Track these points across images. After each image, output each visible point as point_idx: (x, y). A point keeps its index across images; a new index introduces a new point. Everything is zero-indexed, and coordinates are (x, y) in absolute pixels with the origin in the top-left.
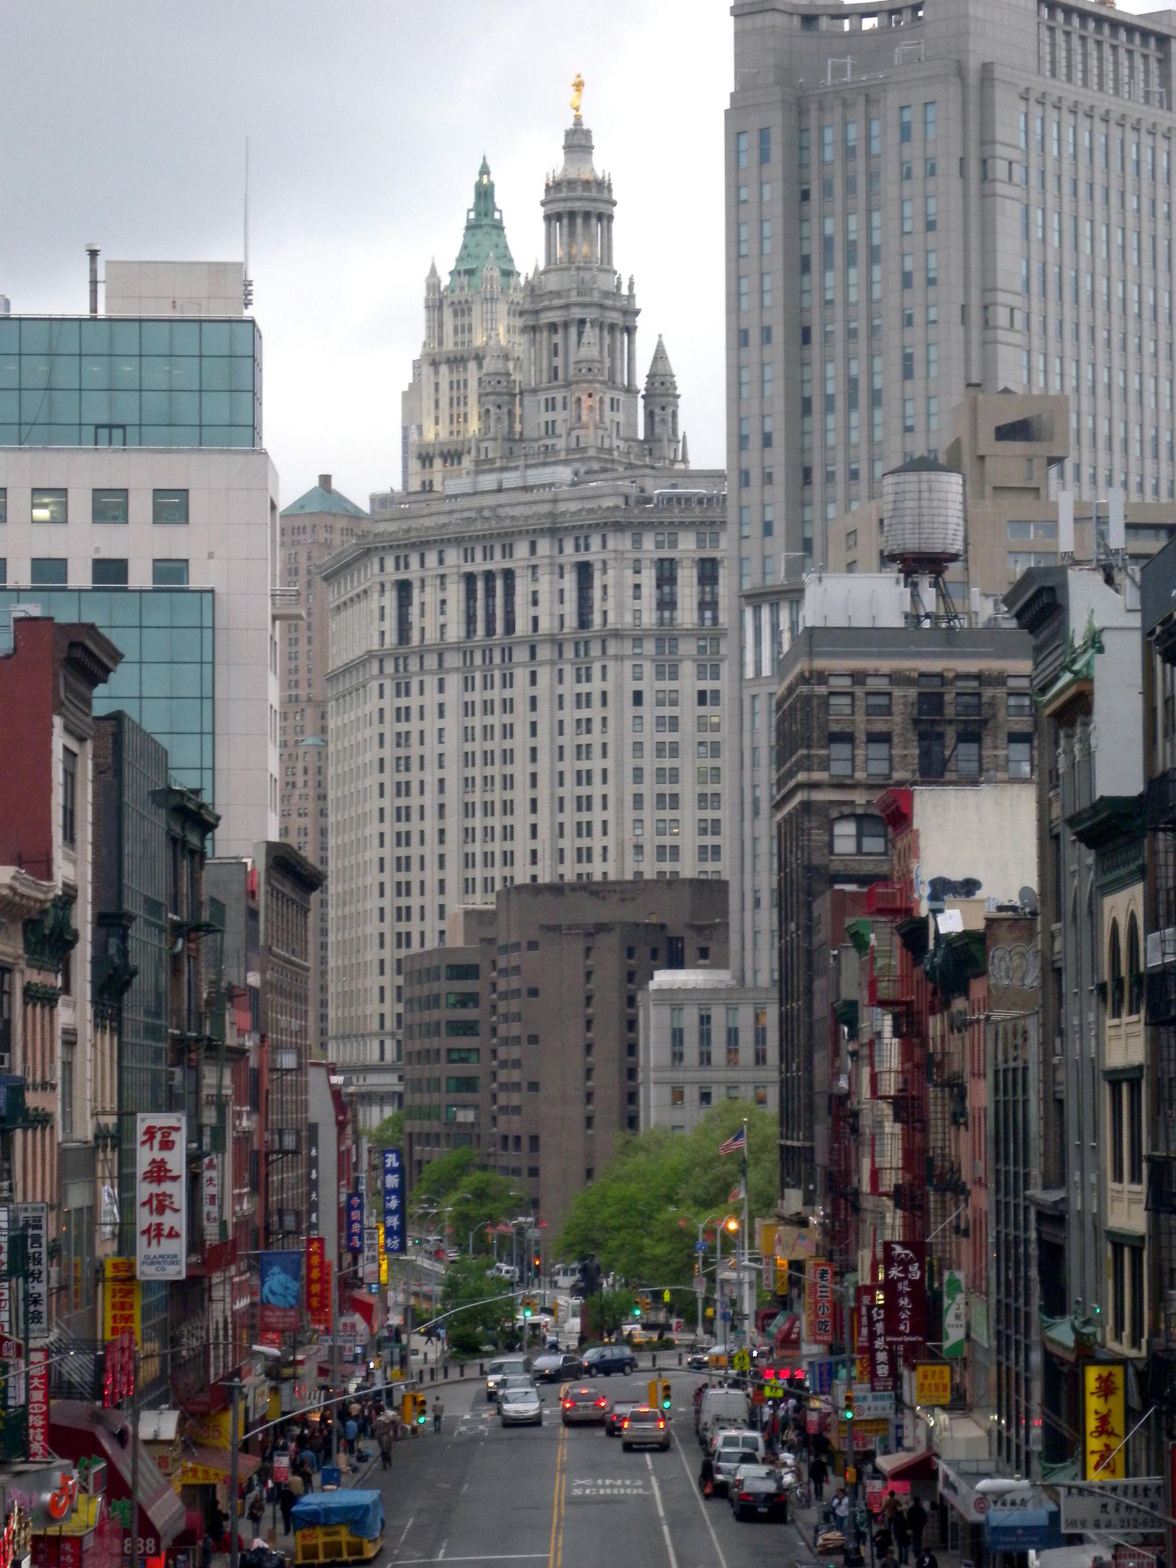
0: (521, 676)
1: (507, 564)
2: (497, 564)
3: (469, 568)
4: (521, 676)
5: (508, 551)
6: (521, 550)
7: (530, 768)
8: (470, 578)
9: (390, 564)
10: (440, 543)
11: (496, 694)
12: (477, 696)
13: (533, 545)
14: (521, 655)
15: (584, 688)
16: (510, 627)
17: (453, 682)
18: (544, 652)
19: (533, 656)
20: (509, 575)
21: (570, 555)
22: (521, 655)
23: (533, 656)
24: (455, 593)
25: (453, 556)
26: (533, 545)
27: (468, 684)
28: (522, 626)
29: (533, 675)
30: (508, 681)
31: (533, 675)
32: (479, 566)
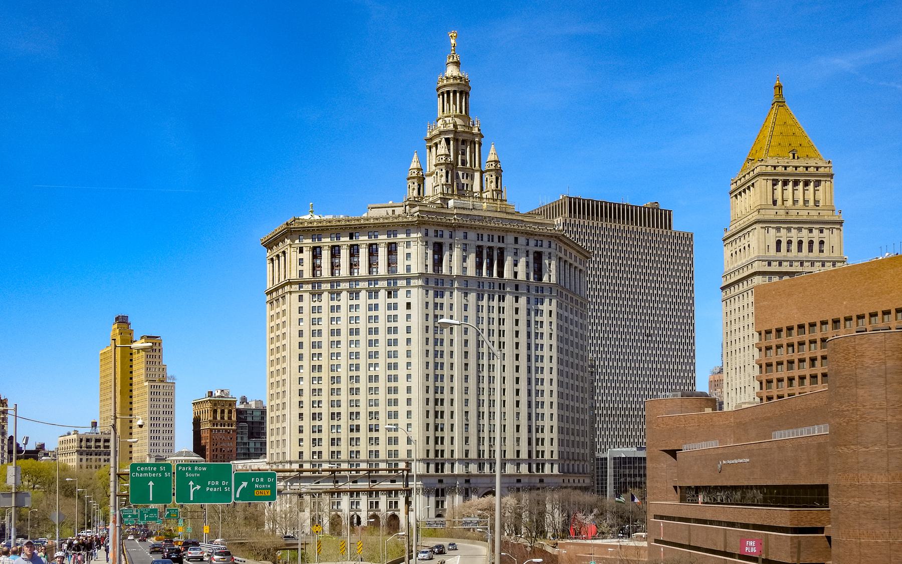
1: (501, 245)
2: (496, 244)
3: (480, 243)
5: (501, 239)
6: (510, 239)
13: (516, 239)
21: (532, 248)
26: (516, 239)
30: (502, 298)
32: (485, 243)
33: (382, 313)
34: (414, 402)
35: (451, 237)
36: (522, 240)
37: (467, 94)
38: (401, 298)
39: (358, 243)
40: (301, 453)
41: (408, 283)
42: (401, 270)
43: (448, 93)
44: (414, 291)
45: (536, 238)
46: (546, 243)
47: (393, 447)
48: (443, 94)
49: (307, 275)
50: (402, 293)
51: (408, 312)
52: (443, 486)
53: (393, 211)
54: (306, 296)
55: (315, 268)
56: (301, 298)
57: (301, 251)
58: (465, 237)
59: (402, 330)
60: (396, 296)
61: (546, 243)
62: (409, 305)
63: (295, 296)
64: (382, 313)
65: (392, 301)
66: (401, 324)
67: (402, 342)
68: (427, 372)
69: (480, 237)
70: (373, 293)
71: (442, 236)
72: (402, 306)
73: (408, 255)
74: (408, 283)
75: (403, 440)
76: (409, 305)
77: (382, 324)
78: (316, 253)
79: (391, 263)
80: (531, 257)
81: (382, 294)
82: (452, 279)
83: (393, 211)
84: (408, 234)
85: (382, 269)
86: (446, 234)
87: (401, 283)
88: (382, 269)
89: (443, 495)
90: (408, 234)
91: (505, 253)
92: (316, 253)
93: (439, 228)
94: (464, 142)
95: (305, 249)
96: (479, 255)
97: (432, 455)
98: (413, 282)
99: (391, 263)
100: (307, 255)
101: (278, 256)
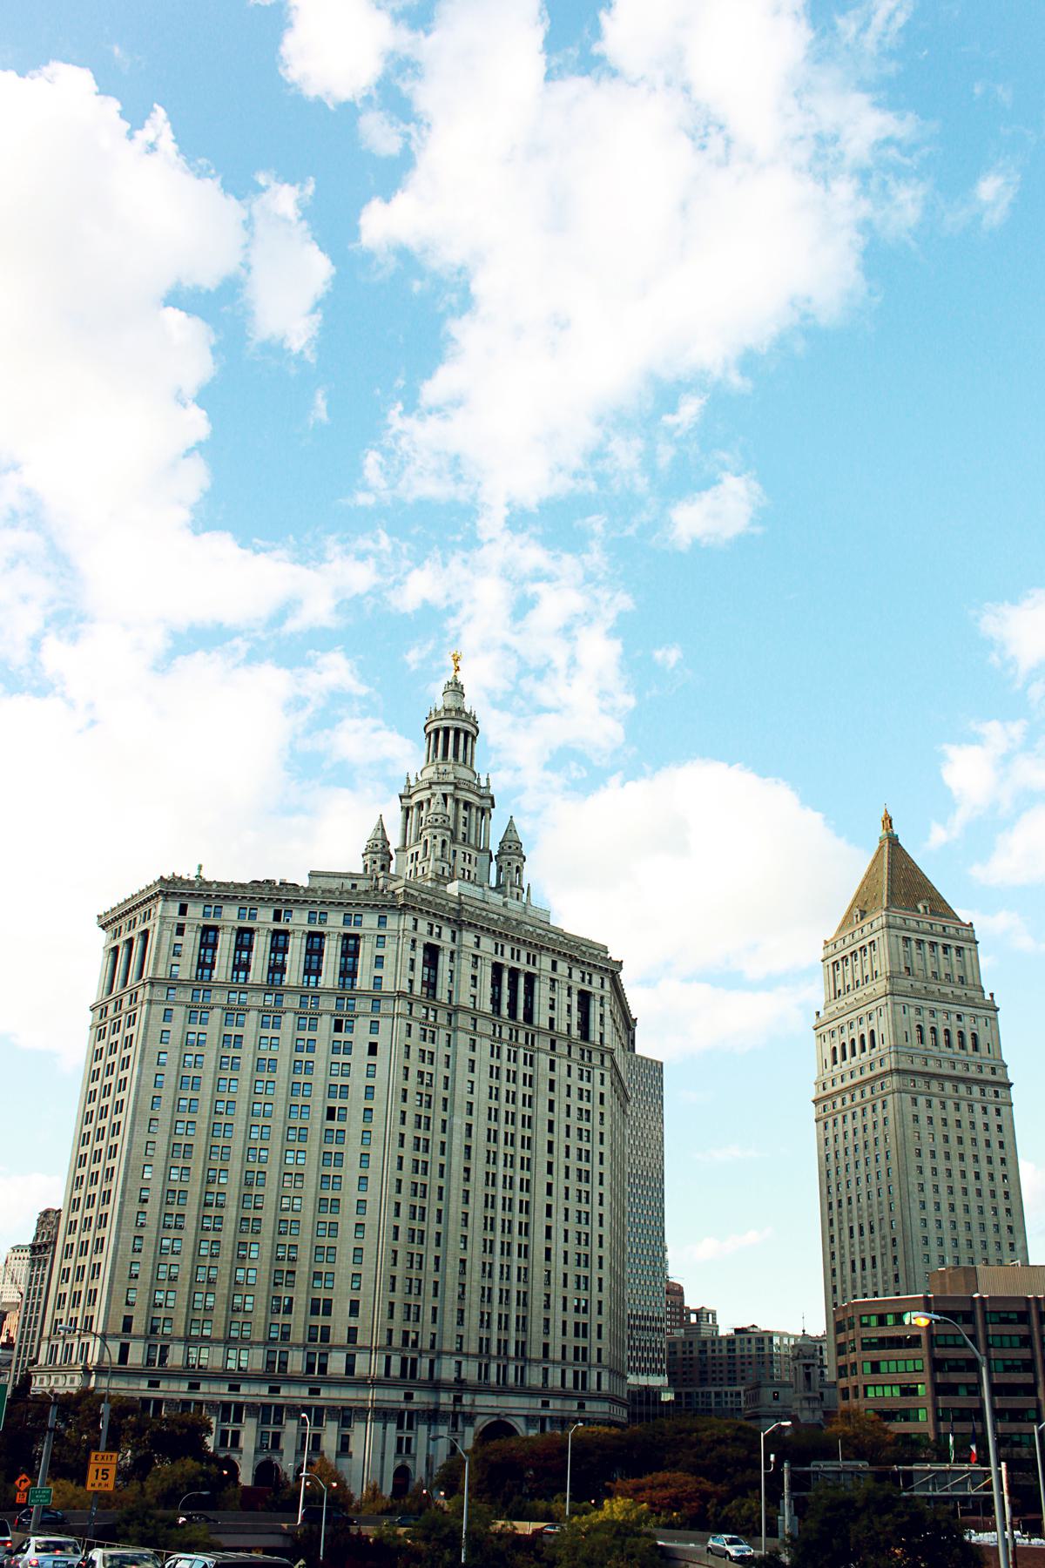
0: (543, 1060)
2: (522, 965)
4: (543, 1060)
5: (531, 960)
6: (545, 962)
7: (548, 1137)
8: (497, 968)
9: (423, 926)
10: (482, 929)
11: (524, 1069)
12: (505, 1065)
13: (554, 964)
14: (543, 1042)
15: (585, 1085)
16: (529, 1017)
17: (484, 1045)
18: (562, 1047)
19: (553, 1048)
20: (530, 978)
22: (543, 1042)
23: (553, 1048)
24: (486, 975)
25: (487, 944)
26: (554, 968)
27: (495, 1052)
28: (541, 1019)
29: (552, 1063)
31: (552, 1063)
32: (507, 960)
33: (321, 1057)
34: (370, 1232)
35: (453, 940)
36: (563, 967)
37: (474, 738)
38: (360, 1034)
39: (290, 928)
40: (128, 1323)
41: (375, 1009)
42: (363, 981)
43: (447, 730)
44: (385, 1024)
45: (583, 968)
46: (596, 980)
47: (320, 1320)
48: (437, 731)
49: (186, 970)
50: (362, 1025)
51: (372, 1060)
52: (411, 1407)
53: (354, 886)
54: (179, 1013)
55: (205, 965)
56: (167, 1016)
57: (180, 930)
58: (478, 945)
59: (356, 1092)
60: (350, 1029)
61: (596, 980)
62: (373, 1049)
63: (158, 1010)
64: (321, 1057)
65: (342, 1036)
66: (357, 1082)
67: (355, 1114)
68: (398, 1175)
69: (499, 949)
70: (309, 1019)
71: (439, 935)
72: (361, 1049)
73: (379, 962)
74: (375, 1009)
75: (341, 1308)
76: (373, 1049)
77: (319, 1079)
78: (209, 936)
79: (348, 973)
80: (575, 997)
81: (326, 1023)
82: (454, 1010)
83: (354, 886)
84: (382, 921)
85: (329, 976)
86: (447, 933)
87: (363, 1005)
88: (329, 976)
89: (410, 1427)
90: (382, 921)
91: (537, 985)
92: (209, 936)
93: (435, 922)
94: (467, 805)
95: (187, 929)
96: (496, 982)
97: (397, 1340)
98: (386, 1006)
99: (348, 973)
100: (191, 939)
101: (130, 942)
